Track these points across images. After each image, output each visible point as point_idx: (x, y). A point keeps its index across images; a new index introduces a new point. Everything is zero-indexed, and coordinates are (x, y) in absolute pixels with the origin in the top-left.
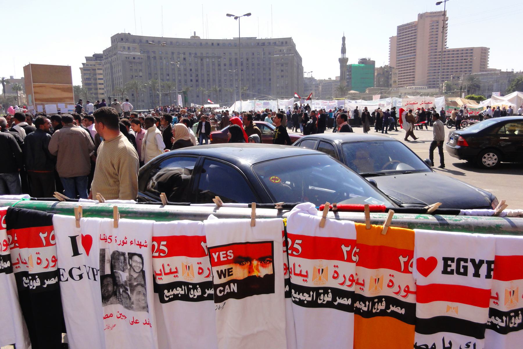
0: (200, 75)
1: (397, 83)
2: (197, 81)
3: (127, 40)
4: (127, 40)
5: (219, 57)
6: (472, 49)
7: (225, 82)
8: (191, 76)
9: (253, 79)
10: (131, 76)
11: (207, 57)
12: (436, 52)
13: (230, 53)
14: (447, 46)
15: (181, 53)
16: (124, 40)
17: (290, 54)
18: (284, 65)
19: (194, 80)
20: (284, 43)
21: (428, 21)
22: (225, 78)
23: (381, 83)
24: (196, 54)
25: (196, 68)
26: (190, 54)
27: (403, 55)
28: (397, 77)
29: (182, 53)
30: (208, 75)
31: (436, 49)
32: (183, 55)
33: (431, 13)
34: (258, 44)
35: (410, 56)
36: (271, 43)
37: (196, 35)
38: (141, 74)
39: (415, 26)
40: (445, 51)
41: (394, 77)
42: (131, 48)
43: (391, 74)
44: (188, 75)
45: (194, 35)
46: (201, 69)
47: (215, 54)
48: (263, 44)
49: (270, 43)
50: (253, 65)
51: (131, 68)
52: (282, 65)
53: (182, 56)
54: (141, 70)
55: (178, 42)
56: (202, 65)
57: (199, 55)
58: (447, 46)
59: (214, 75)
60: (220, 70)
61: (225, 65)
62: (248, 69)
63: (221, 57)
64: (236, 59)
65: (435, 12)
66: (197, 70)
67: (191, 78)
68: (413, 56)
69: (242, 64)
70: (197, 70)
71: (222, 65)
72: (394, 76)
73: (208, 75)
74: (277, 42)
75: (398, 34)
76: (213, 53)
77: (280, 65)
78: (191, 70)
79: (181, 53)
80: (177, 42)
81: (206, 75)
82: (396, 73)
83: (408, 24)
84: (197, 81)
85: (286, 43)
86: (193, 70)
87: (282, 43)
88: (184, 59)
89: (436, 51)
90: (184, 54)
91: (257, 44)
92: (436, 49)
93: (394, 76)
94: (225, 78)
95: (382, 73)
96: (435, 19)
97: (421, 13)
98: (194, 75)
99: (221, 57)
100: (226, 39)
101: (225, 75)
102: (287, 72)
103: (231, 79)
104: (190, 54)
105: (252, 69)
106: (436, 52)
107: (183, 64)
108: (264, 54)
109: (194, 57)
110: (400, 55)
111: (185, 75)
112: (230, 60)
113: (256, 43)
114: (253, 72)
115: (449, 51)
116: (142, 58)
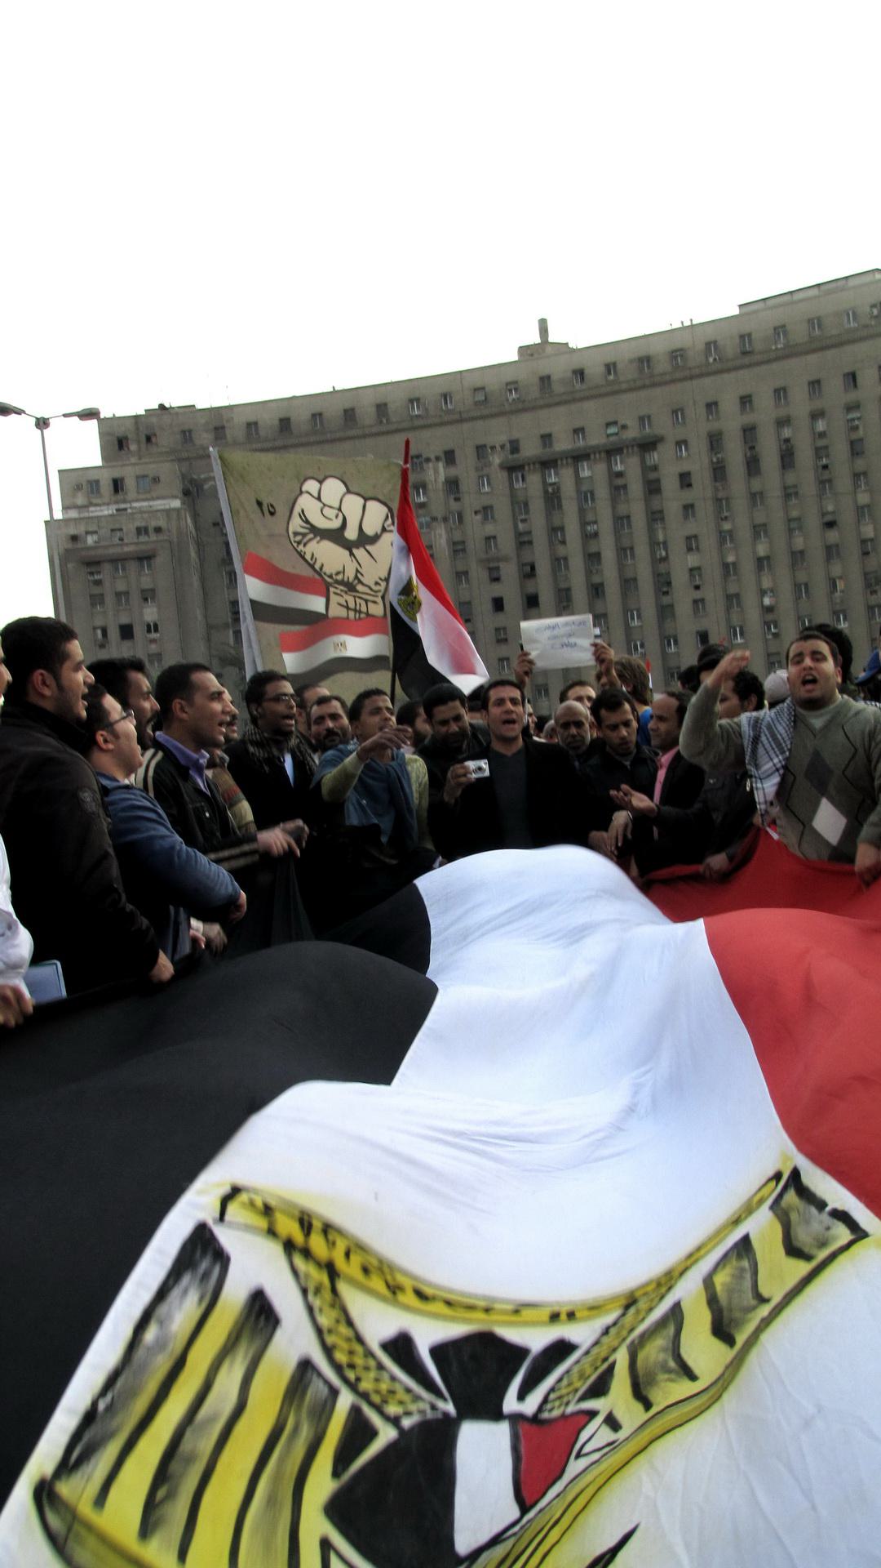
3: (148, 439)
4: (148, 439)
5: (648, 445)
7: (697, 588)
8: (497, 579)
9: (864, 542)
10: (99, 632)
15: (428, 460)
16: (133, 447)
22: (692, 560)
24: (515, 447)
25: (521, 526)
26: (481, 450)
29: (438, 459)
32: (441, 465)
38: (150, 614)
42: (130, 483)
45: (538, 340)
47: (624, 427)
51: (96, 590)
53: (436, 474)
54: (147, 596)
55: (418, 400)
56: (553, 499)
57: (531, 449)
60: (656, 517)
61: (685, 480)
62: (830, 481)
64: (749, 432)
67: (497, 590)
69: (787, 457)
71: (670, 484)
76: (608, 425)
79: (428, 460)
80: (411, 401)
88: (453, 485)
90: (450, 457)
91: (875, 312)
94: (692, 560)
100: (687, 323)
101: (692, 543)
103: (731, 559)
104: (481, 450)
107: (445, 519)
109: (502, 467)
112: (715, 441)
113: (874, 306)
116: (158, 530)
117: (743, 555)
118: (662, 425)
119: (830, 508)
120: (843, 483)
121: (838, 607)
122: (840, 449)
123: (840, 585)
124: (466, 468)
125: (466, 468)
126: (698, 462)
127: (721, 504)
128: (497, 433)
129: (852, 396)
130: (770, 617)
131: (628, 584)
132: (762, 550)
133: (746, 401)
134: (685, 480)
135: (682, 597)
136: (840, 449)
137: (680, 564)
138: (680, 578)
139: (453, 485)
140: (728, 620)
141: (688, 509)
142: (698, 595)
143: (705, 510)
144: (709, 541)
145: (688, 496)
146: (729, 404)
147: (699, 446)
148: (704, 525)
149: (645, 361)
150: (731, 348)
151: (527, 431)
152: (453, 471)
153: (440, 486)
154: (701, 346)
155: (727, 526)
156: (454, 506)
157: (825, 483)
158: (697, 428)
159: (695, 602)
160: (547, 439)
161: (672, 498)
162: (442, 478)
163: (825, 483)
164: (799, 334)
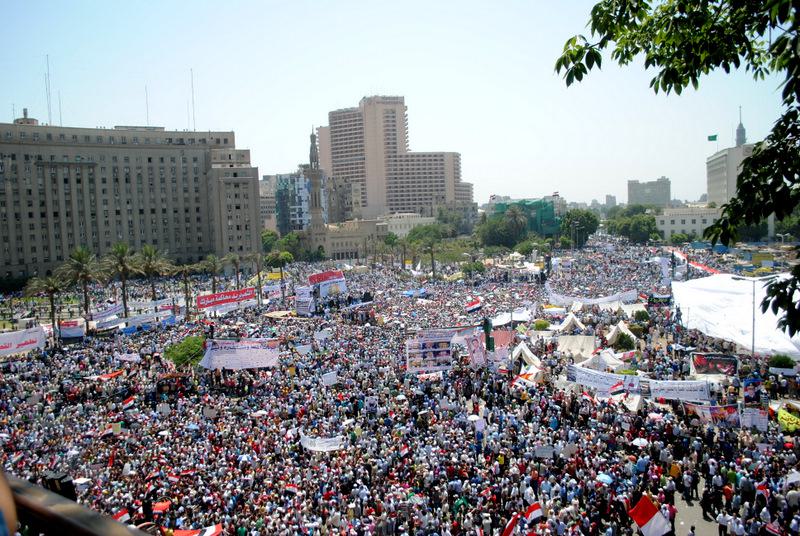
0: (49, 204)
1: (361, 204)
2: (43, 215)
5: (92, 166)
6: (442, 155)
11: (68, 165)
13: (115, 159)
19: (37, 215)
20: (222, 142)
21: (381, 108)
22: (105, 207)
24: (40, 158)
30: (68, 203)
32: (10, 159)
33: (384, 98)
34: (170, 140)
36: (197, 142)
37: (29, 117)
39: (360, 115)
40: (407, 156)
43: (350, 191)
44: (23, 202)
46: (69, 194)
48: (181, 142)
49: (193, 140)
50: (163, 181)
59: (81, 202)
61: (104, 181)
65: (389, 98)
66: (42, 193)
70: (42, 193)
71: (98, 181)
73: (68, 203)
74: (208, 140)
75: (331, 124)
78: (30, 192)
81: (62, 204)
83: (347, 111)
84: (43, 215)
85: (226, 141)
86: (35, 192)
87: (218, 141)
90: (13, 157)
92: (395, 152)
96: (389, 107)
97: (368, 96)
98: (36, 203)
101: (105, 202)
106: (395, 156)
108: (184, 161)
111: (17, 203)
112: (115, 169)
114: (163, 196)
115: (412, 156)
117: (125, 208)
118: (97, 160)
120: (158, 190)
122: (157, 180)
124: (20, 161)
125: (20, 161)
126: (109, 176)
127: (117, 193)
128: (34, 151)
129: (162, 165)
131: (82, 213)
132: (129, 207)
133: (127, 159)
134: (104, 181)
135: (101, 221)
136: (157, 180)
137: (101, 209)
138: (100, 213)
139: (15, 168)
141: (104, 191)
143: (110, 192)
144: (111, 202)
145: (104, 186)
146: (121, 158)
147: (109, 171)
148: (109, 196)
149: (87, 138)
150: (118, 140)
151: (59, 154)
152: (14, 162)
153: (9, 168)
154: (107, 137)
155: (117, 198)
156: (15, 176)
157: (152, 190)
158: (109, 164)
160: (52, 157)
161: (99, 186)
162: (10, 164)
163: (152, 190)
164: (142, 141)
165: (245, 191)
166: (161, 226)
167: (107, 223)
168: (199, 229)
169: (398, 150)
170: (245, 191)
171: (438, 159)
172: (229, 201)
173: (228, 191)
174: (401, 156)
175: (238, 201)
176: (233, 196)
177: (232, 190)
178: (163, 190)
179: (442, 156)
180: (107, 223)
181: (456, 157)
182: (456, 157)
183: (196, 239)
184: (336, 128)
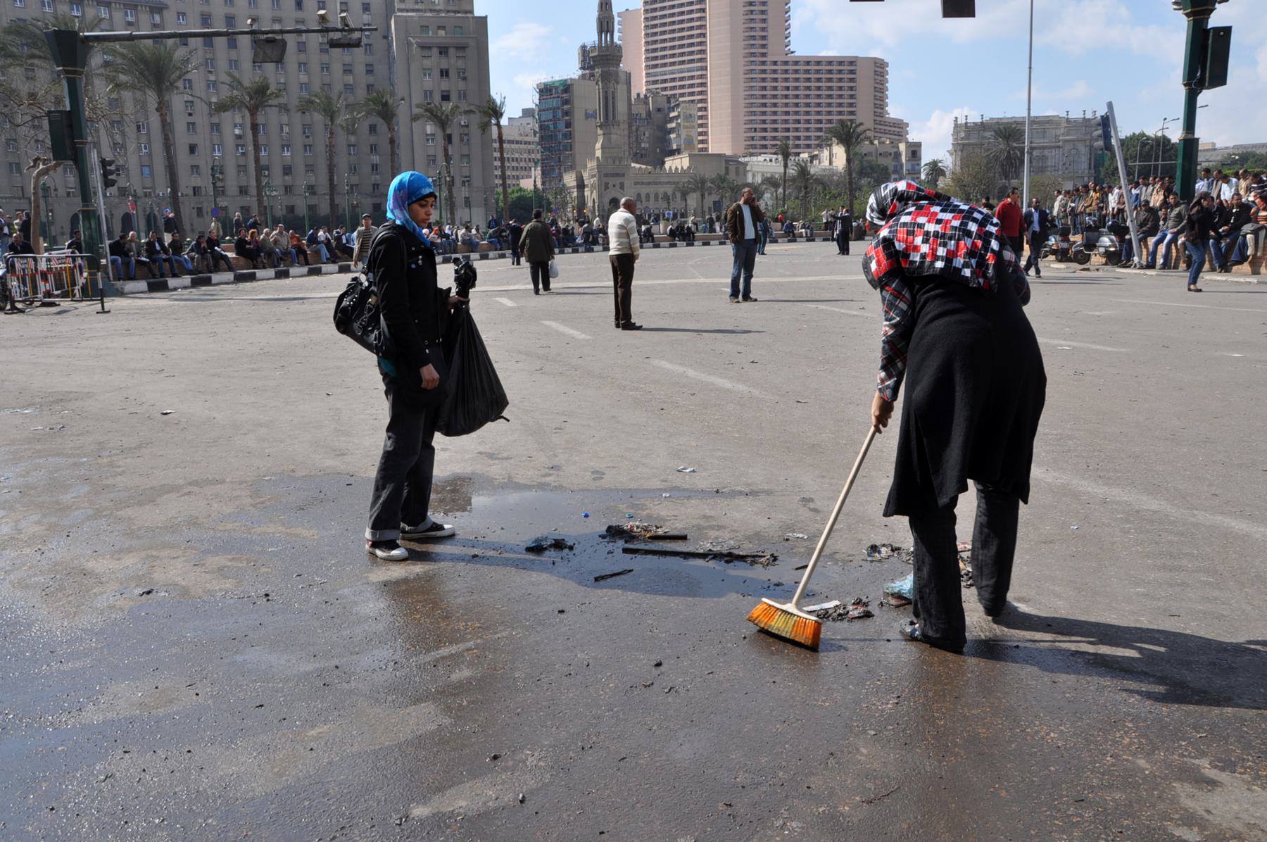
6: (852, 62)
7: (190, 115)
12: (763, 63)
14: (792, 48)
17: (459, 12)
18: (452, 51)
23: (643, 145)
27: (665, 65)
28: (693, 127)
31: (764, 55)
35: (690, 70)
40: (786, 63)
41: (687, 127)
52: (443, 50)
58: (792, 48)
63: (166, 7)
68: (698, 70)
72: (686, 124)
77: (435, 51)
82: (690, 115)
89: (764, 59)
92: (764, 55)
93: (686, 124)
95: (644, 115)
99: (166, 7)
102: (465, 79)
105: (300, 64)
106: (763, 63)
110: (655, 66)
115: (796, 63)
119: (282, 81)
121: (284, 143)
123: (286, 129)
130: (240, 142)
140: (211, 140)
142: (191, 119)
159: (188, 123)
165: (460, 64)
166: (299, 141)
167: (191, 126)
168: (374, 149)
169: (769, 50)
170: (460, 64)
171: (847, 66)
172: (429, 83)
173: (427, 63)
174: (775, 63)
175: (445, 85)
176: (437, 73)
177: (435, 61)
178: (303, 65)
179: (851, 63)
180: (191, 126)
181: (879, 68)
182: (879, 68)
183: (366, 169)
184: (655, 18)
